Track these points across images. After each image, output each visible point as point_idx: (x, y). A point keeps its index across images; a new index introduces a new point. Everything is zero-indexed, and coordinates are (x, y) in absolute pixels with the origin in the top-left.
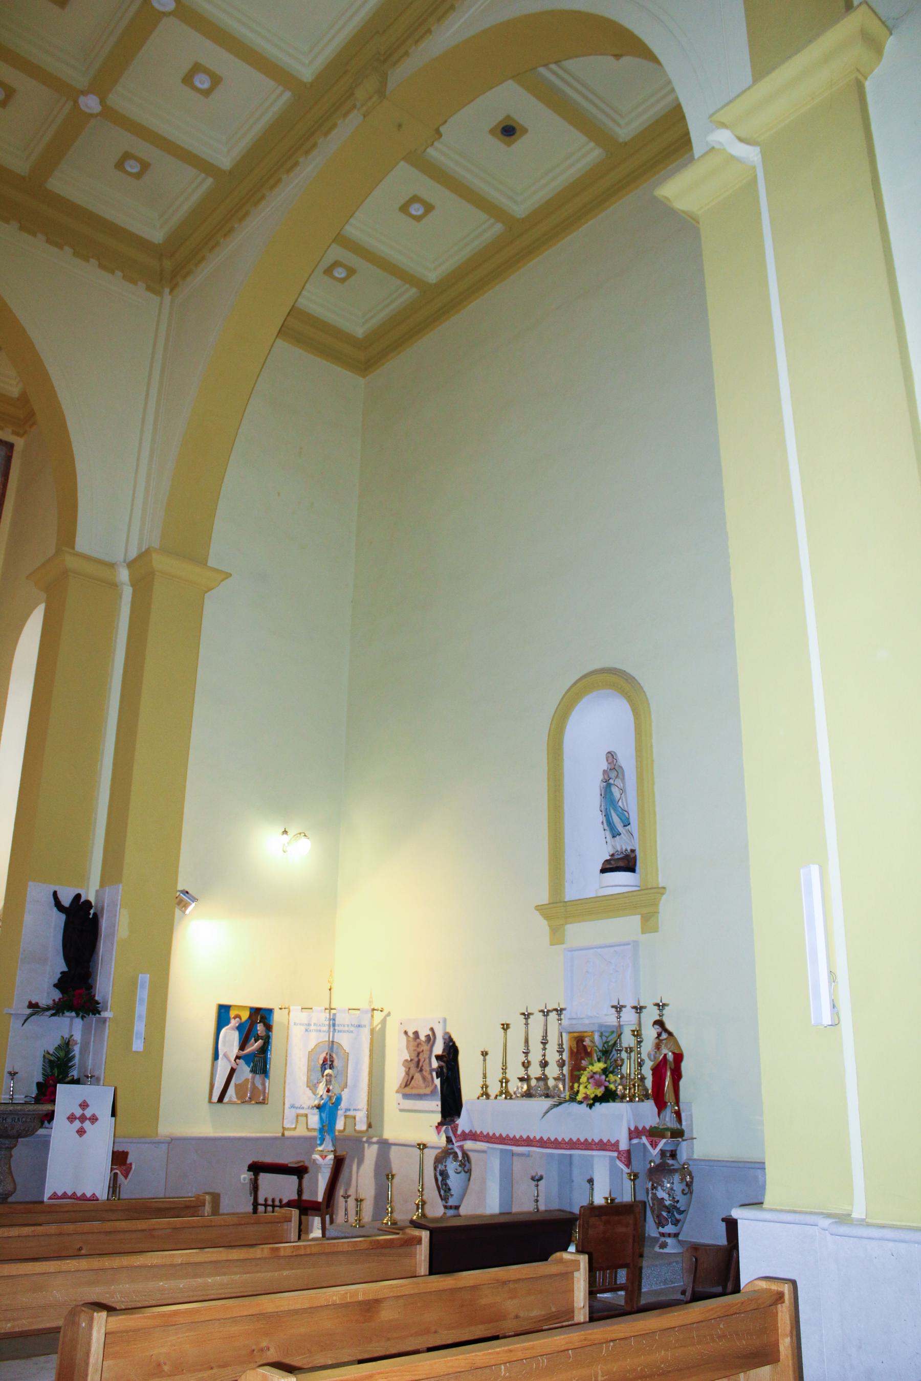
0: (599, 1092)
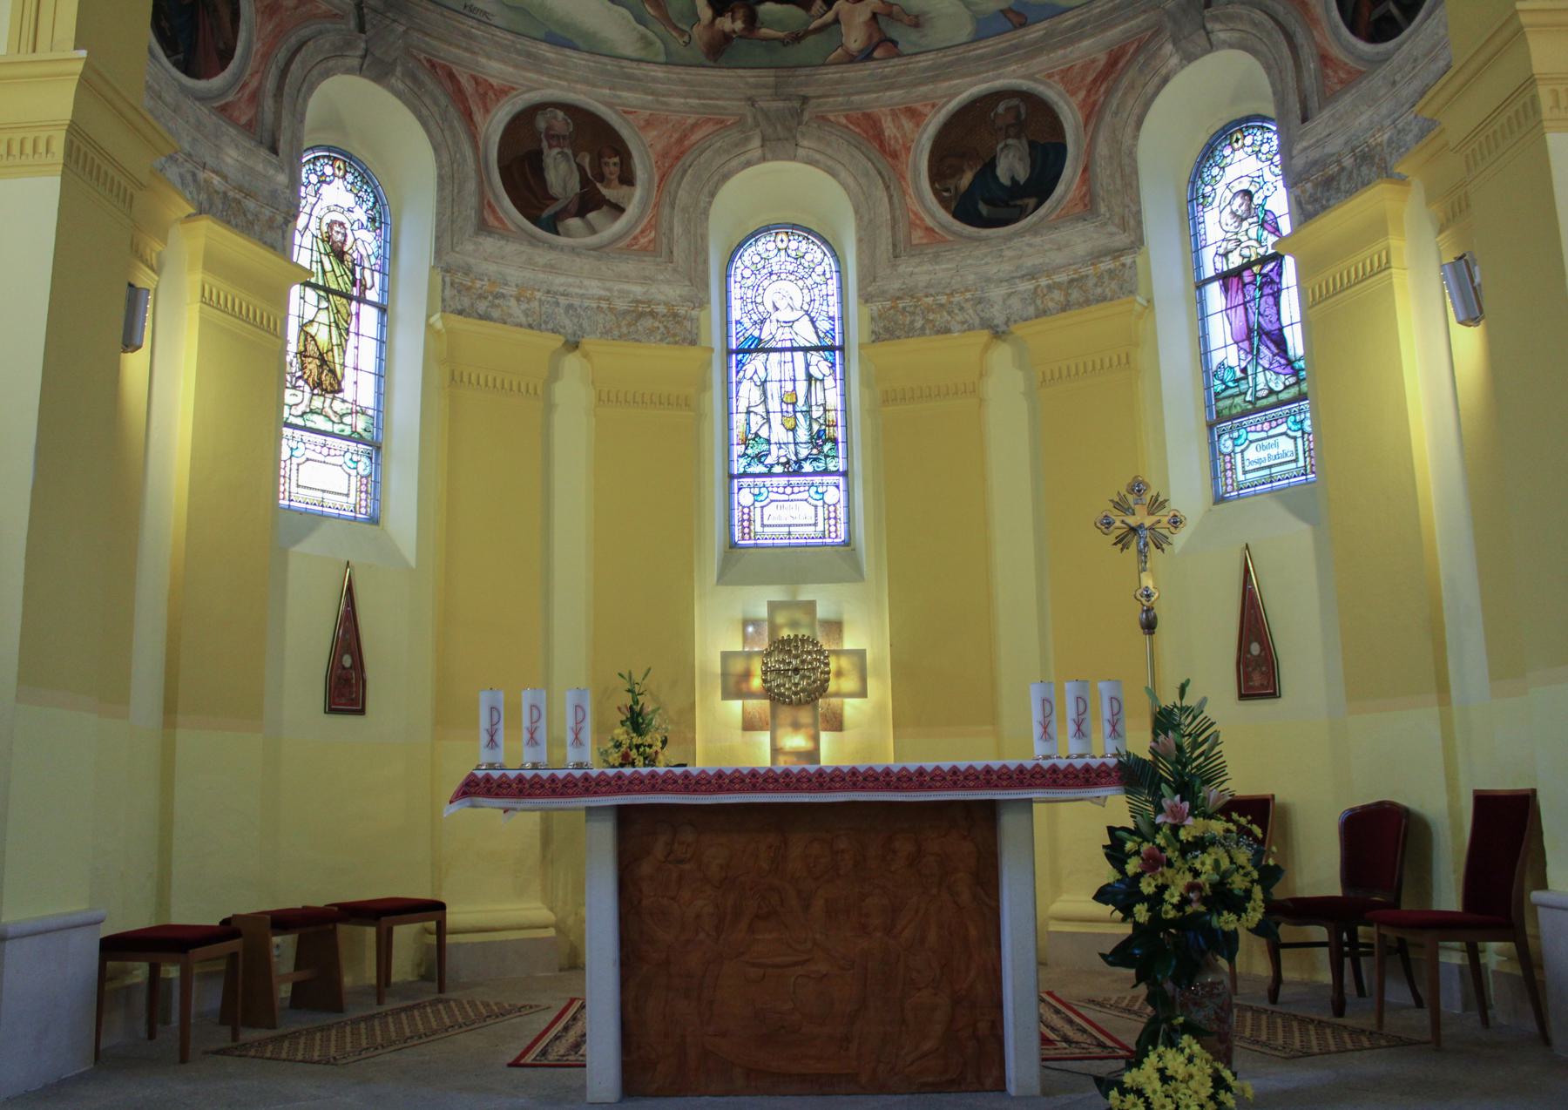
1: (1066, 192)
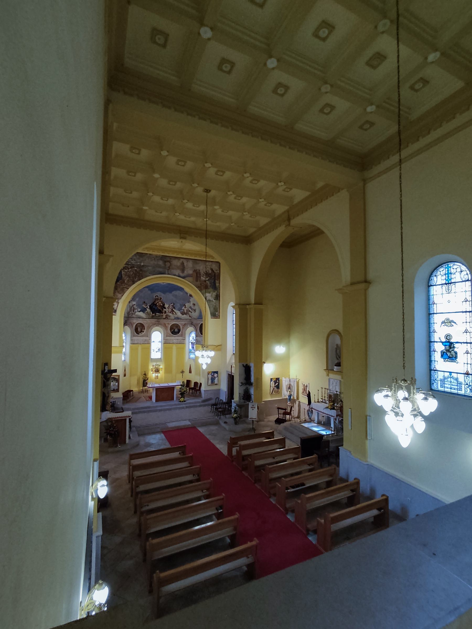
0: (332, 408)
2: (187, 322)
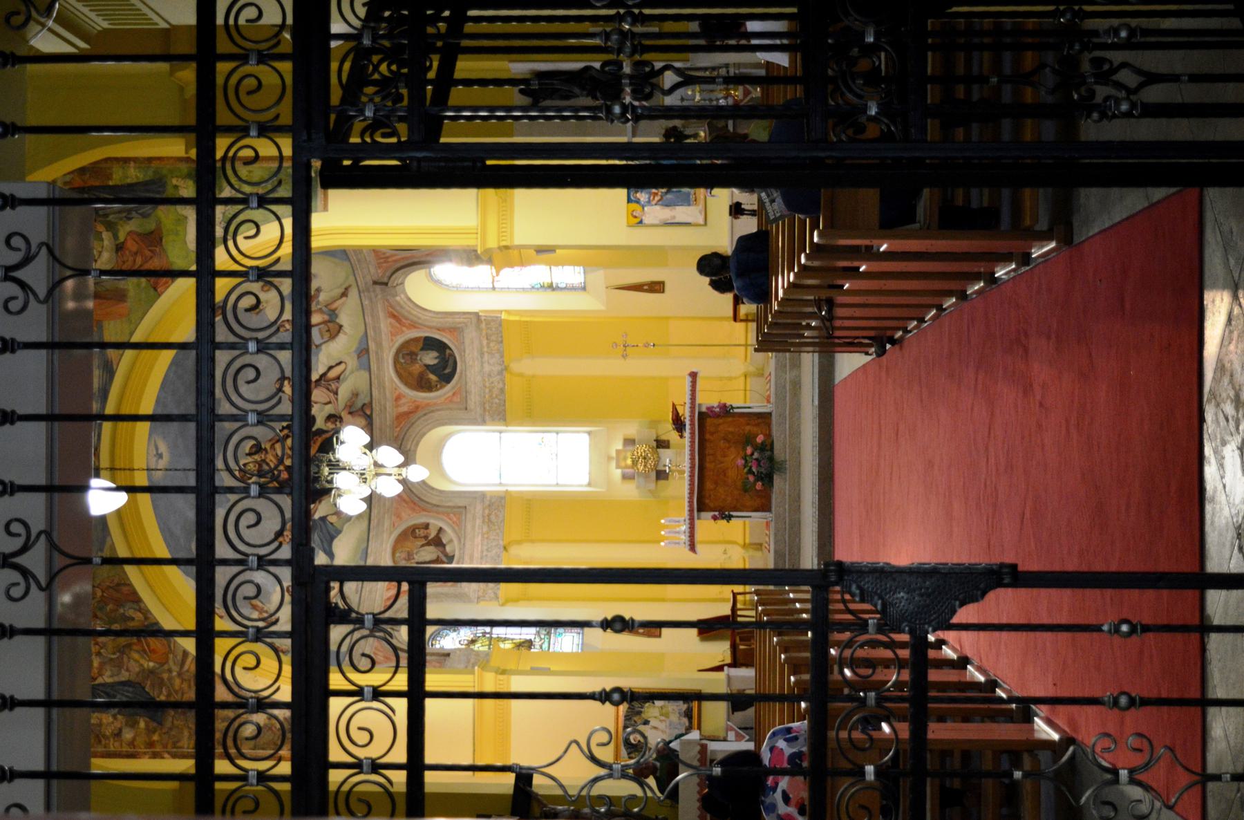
1: (446, 337)
2: (380, 306)
